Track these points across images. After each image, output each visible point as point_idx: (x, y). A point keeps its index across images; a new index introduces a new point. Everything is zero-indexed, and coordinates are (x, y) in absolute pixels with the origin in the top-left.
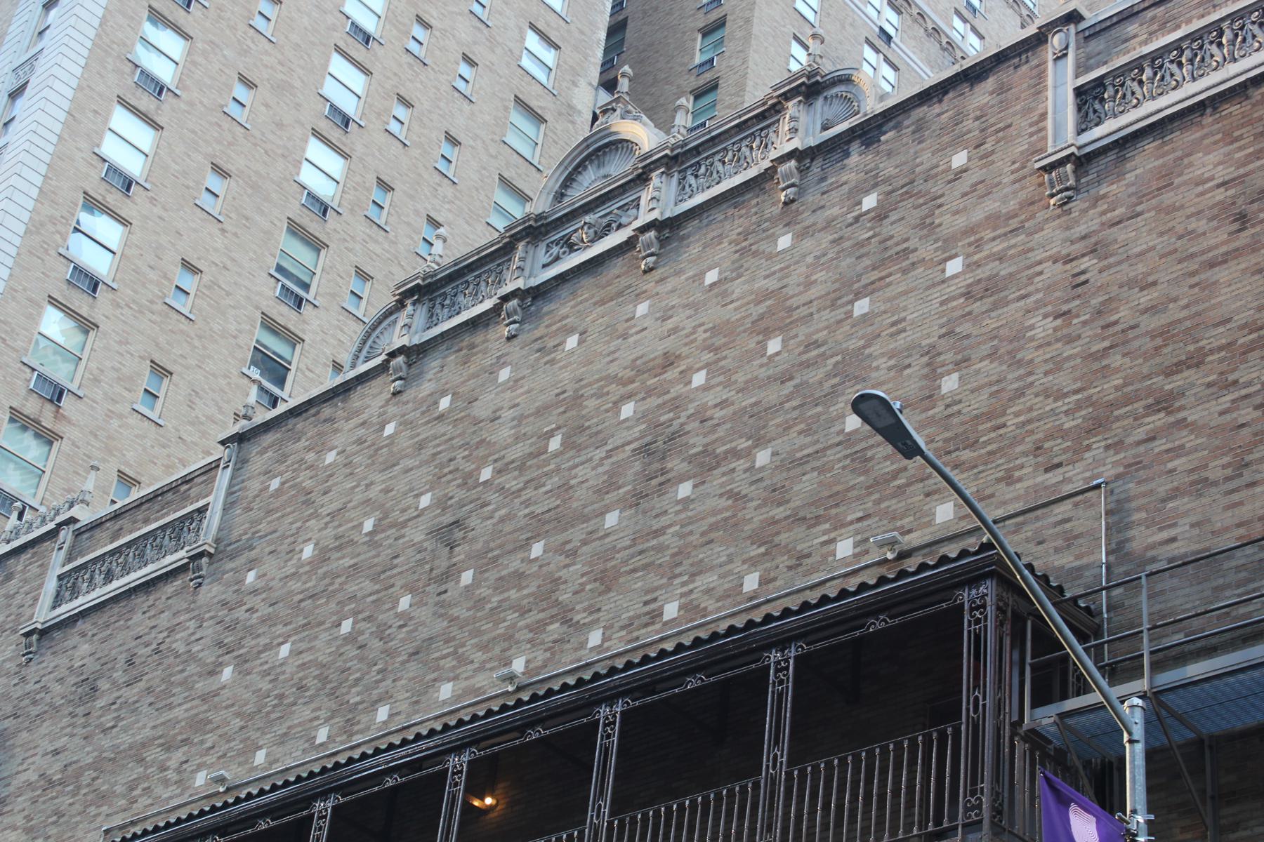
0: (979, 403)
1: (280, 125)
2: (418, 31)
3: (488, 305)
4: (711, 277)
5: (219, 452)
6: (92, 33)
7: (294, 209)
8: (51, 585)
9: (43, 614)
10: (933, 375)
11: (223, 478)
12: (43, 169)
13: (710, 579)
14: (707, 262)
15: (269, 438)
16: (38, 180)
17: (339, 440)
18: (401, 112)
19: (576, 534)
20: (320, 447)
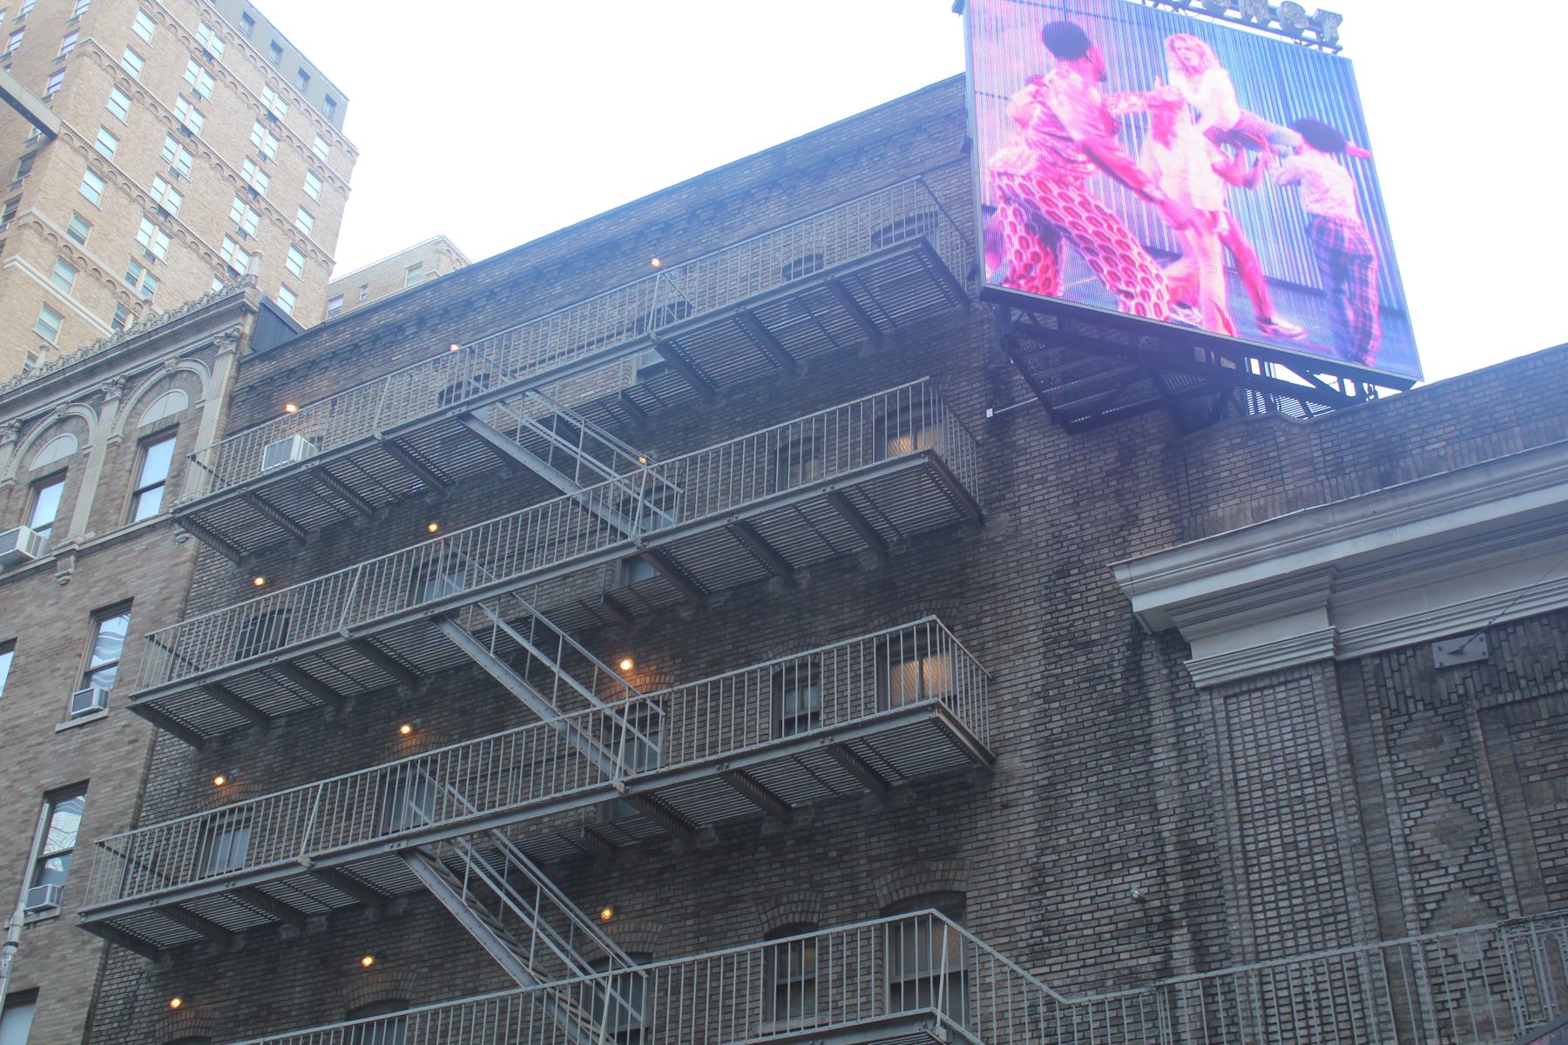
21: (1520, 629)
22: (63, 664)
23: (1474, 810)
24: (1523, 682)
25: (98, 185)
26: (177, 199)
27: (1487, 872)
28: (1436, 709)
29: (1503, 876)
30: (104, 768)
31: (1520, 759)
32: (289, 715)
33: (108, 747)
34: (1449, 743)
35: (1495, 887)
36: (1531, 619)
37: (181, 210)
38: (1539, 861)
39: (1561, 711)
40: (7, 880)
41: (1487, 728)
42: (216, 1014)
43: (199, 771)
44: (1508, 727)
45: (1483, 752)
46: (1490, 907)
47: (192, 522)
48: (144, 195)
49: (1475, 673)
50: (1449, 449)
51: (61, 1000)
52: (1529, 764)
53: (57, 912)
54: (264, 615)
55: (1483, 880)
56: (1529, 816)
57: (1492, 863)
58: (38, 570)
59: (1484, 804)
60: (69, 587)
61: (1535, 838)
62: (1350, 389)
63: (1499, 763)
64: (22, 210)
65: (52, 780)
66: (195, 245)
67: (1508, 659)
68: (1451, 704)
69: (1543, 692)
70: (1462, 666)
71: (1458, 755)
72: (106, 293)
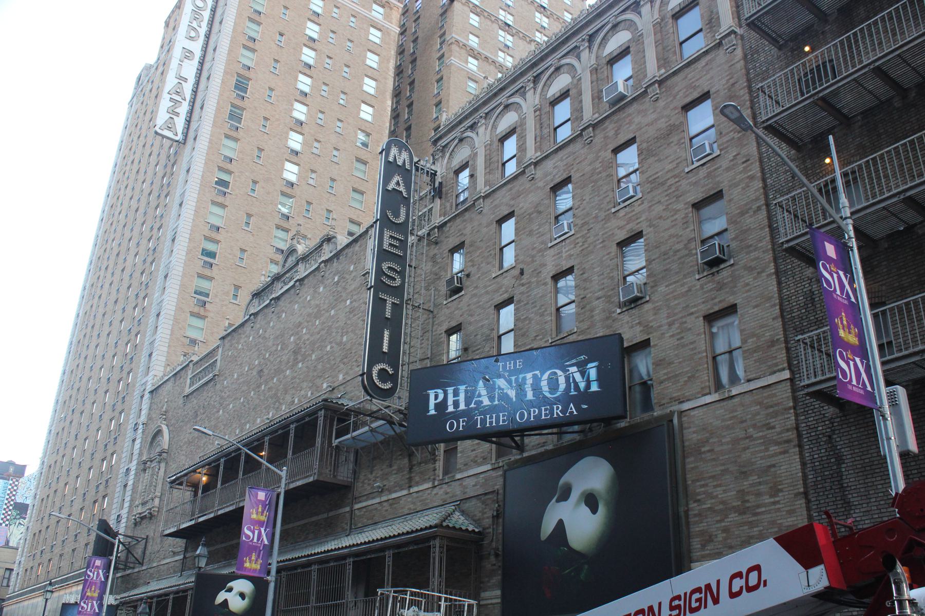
0: (348, 346)
1: (268, 193)
2: (316, 144)
3: (268, 302)
4: (309, 298)
5: (219, 342)
6: (199, 182)
7: (277, 220)
8: (188, 381)
9: (188, 390)
10: (342, 336)
11: (220, 350)
12: (189, 232)
13: (303, 392)
14: (307, 294)
15: (229, 338)
16: (188, 236)
17: (242, 341)
18: (313, 176)
19: (281, 376)
20: (238, 343)
22: (675, 139)
25: (477, 18)
26: (511, 18)
30: (729, 181)
32: (862, 113)
33: (728, 169)
37: (514, 22)
40: (686, 255)
42: (884, 288)
43: (804, 162)
47: (755, 25)
48: (497, 19)
51: (756, 306)
53: (732, 262)
54: (818, 67)
58: (634, 99)
60: (660, 101)
64: (447, 37)
65: (696, 195)
66: (524, 37)
72: (492, 67)
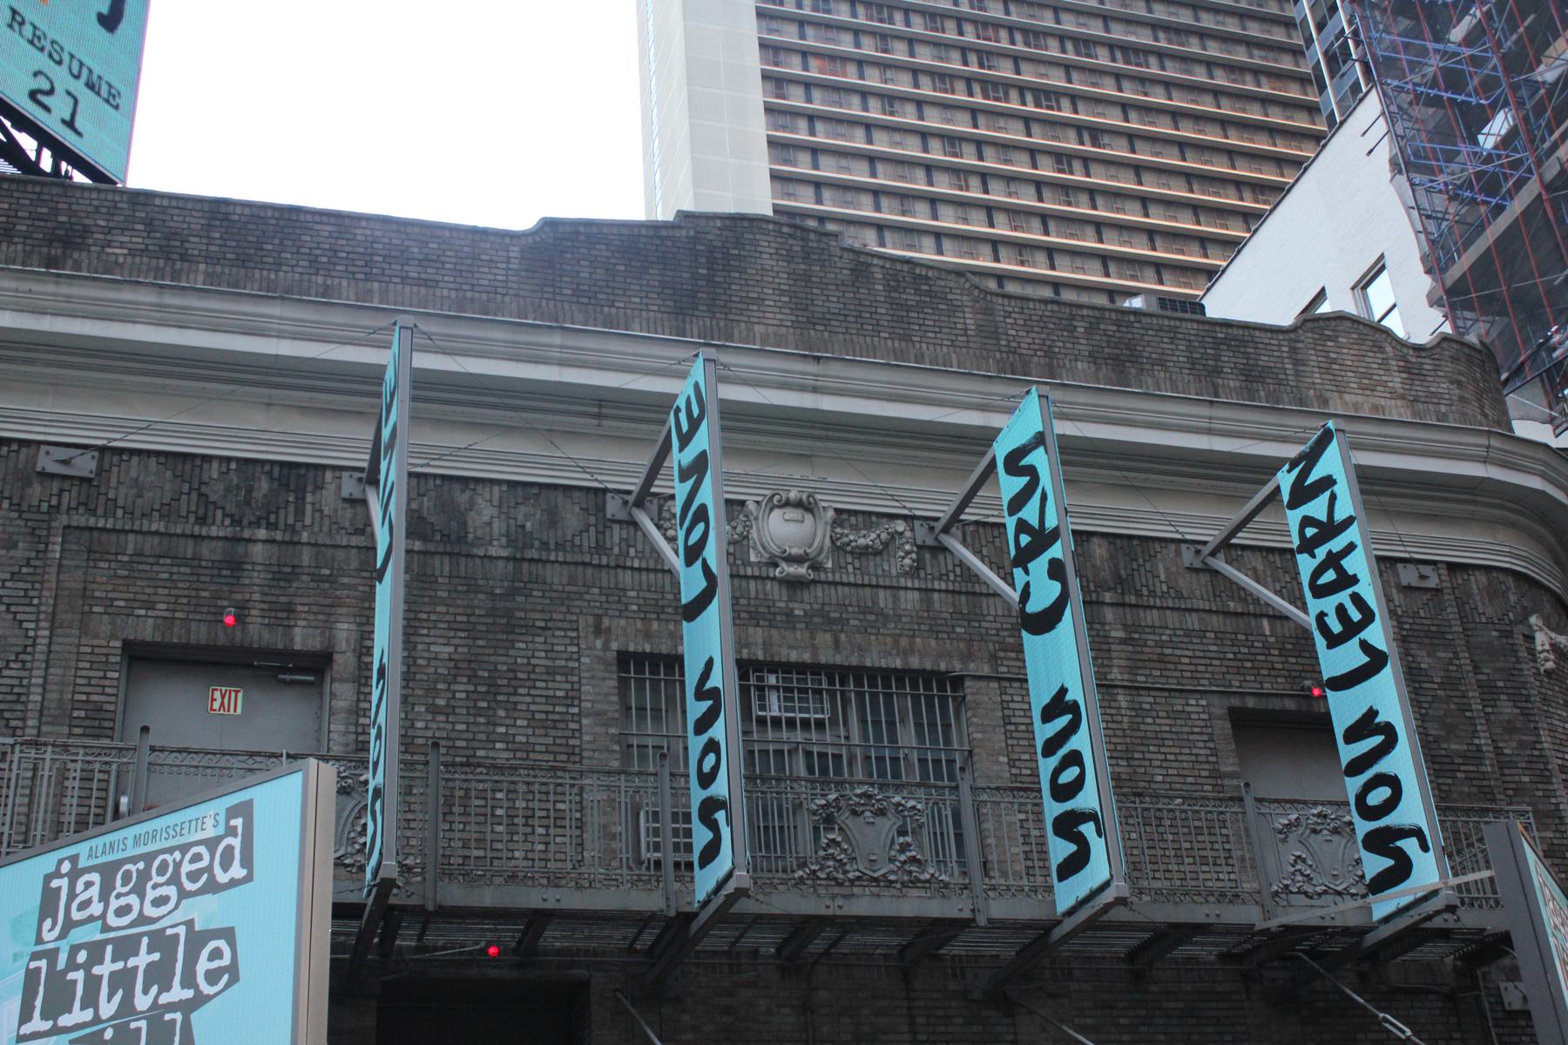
21: (135, 460)
23: (25, 625)
24: (120, 512)
27: (16, 690)
28: (21, 512)
29: (32, 698)
31: (90, 586)
34: (21, 552)
35: (19, 707)
36: (149, 453)
38: (74, 693)
39: (147, 551)
41: (67, 546)
44: (89, 552)
45: (55, 569)
46: (7, 726)
49: (75, 490)
50: (129, 259)
52: (97, 594)
55: (9, 698)
56: (79, 645)
57: (25, 682)
59: (37, 621)
61: (77, 669)
62: (46, 163)
63: (67, 585)
67: (113, 483)
68: (38, 512)
69: (136, 527)
70: (64, 477)
71: (28, 565)
